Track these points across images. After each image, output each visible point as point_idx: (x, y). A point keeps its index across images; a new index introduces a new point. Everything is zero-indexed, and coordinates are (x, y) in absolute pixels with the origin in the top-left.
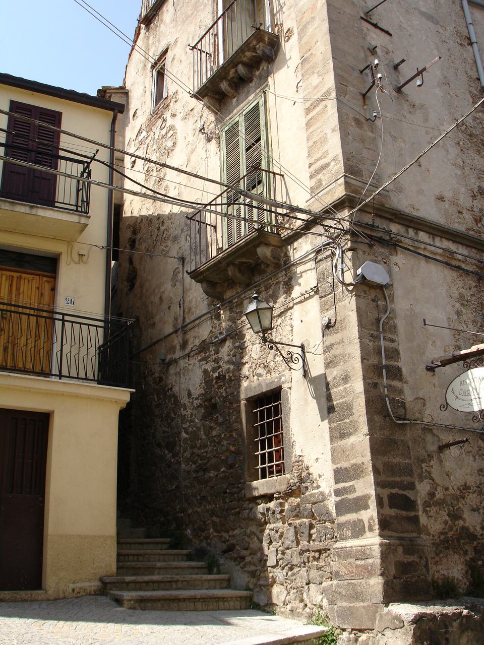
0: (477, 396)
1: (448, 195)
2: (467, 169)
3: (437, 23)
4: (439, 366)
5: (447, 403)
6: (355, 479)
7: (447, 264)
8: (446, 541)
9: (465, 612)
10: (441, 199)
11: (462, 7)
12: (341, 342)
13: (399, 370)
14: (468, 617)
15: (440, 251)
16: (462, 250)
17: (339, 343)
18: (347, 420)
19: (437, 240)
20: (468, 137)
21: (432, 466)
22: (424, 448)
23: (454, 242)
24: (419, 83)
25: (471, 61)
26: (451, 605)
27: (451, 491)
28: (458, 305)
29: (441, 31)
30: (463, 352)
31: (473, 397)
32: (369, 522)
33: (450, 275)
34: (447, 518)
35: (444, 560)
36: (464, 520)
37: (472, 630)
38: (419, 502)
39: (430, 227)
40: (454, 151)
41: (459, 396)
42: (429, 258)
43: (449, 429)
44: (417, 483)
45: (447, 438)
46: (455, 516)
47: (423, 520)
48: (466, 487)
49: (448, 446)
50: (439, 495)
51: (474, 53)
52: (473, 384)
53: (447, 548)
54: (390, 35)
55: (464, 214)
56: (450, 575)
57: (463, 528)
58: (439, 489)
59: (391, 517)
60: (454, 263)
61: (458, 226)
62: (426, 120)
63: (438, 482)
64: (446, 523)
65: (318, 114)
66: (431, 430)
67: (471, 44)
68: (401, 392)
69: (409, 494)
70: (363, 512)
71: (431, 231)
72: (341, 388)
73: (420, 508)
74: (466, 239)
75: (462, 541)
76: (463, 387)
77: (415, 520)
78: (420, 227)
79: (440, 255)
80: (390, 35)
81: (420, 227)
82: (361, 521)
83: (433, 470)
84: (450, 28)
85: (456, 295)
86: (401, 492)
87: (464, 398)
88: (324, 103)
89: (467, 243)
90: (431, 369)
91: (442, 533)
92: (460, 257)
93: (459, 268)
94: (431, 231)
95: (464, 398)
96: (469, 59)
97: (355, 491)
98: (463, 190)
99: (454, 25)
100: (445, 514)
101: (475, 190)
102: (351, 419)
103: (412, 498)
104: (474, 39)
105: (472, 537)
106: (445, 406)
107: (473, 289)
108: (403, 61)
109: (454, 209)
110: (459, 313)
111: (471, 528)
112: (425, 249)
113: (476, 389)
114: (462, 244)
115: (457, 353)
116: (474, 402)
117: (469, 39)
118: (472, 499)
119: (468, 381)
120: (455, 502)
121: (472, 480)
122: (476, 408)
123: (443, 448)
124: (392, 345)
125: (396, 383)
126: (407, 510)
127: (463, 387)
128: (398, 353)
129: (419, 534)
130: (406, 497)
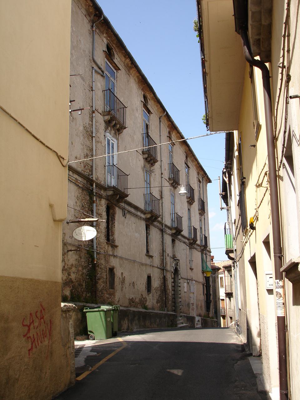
0: (84, 236)
2: (84, 145)
3: (84, 81)
4: (71, 222)
5: (73, 236)
7: (76, 184)
8: (66, 283)
9: (74, 306)
11: (92, 73)
14: (75, 307)
15: (74, 179)
16: (80, 179)
19: (74, 174)
20: (86, 132)
21: (65, 257)
23: (78, 175)
24: (79, 113)
25: (91, 98)
26: (70, 303)
27: (69, 266)
28: (76, 199)
29: (85, 84)
30: (82, 220)
31: (83, 236)
33: (76, 188)
34: (67, 275)
35: (66, 289)
36: (71, 276)
37: (76, 312)
39: (74, 170)
40: (82, 138)
41: (77, 234)
42: (72, 181)
43: (70, 244)
45: (70, 248)
46: (69, 275)
48: (72, 265)
49: (71, 251)
50: (66, 267)
51: (92, 94)
52: (83, 231)
53: (66, 285)
55: (82, 164)
56: (67, 294)
57: (71, 279)
58: (66, 265)
60: (77, 183)
61: (79, 169)
62: (76, 125)
63: (66, 262)
64: (67, 276)
66: (66, 245)
67: (92, 90)
71: (73, 171)
74: (82, 175)
75: (70, 283)
76: (80, 232)
78: (71, 170)
79: (74, 180)
81: (71, 170)
83: (65, 258)
84: (87, 83)
85: (76, 196)
87: (79, 235)
89: (82, 176)
90: (68, 223)
91: (65, 280)
92: (79, 181)
93: (78, 185)
94: (73, 171)
95: (79, 235)
96: (90, 97)
98: (82, 154)
99: (89, 81)
100: (67, 273)
101: (86, 155)
104: (94, 89)
105: (72, 282)
106: (72, 237)
107: (81, 194)
108: (74, 101)
110: (76, 203)
111: (73, 279)
112: (71, 178)
113: (84, 233)
114: (80, 176)
115: (79, 220)
116: (83, 237)
117: (92, 88)
118: (74, 269)
119: (82, 230)
120: (69, 270)
121: (74, 263)
122: (84, 240)
123: (68, 251)
127: (80, 232)
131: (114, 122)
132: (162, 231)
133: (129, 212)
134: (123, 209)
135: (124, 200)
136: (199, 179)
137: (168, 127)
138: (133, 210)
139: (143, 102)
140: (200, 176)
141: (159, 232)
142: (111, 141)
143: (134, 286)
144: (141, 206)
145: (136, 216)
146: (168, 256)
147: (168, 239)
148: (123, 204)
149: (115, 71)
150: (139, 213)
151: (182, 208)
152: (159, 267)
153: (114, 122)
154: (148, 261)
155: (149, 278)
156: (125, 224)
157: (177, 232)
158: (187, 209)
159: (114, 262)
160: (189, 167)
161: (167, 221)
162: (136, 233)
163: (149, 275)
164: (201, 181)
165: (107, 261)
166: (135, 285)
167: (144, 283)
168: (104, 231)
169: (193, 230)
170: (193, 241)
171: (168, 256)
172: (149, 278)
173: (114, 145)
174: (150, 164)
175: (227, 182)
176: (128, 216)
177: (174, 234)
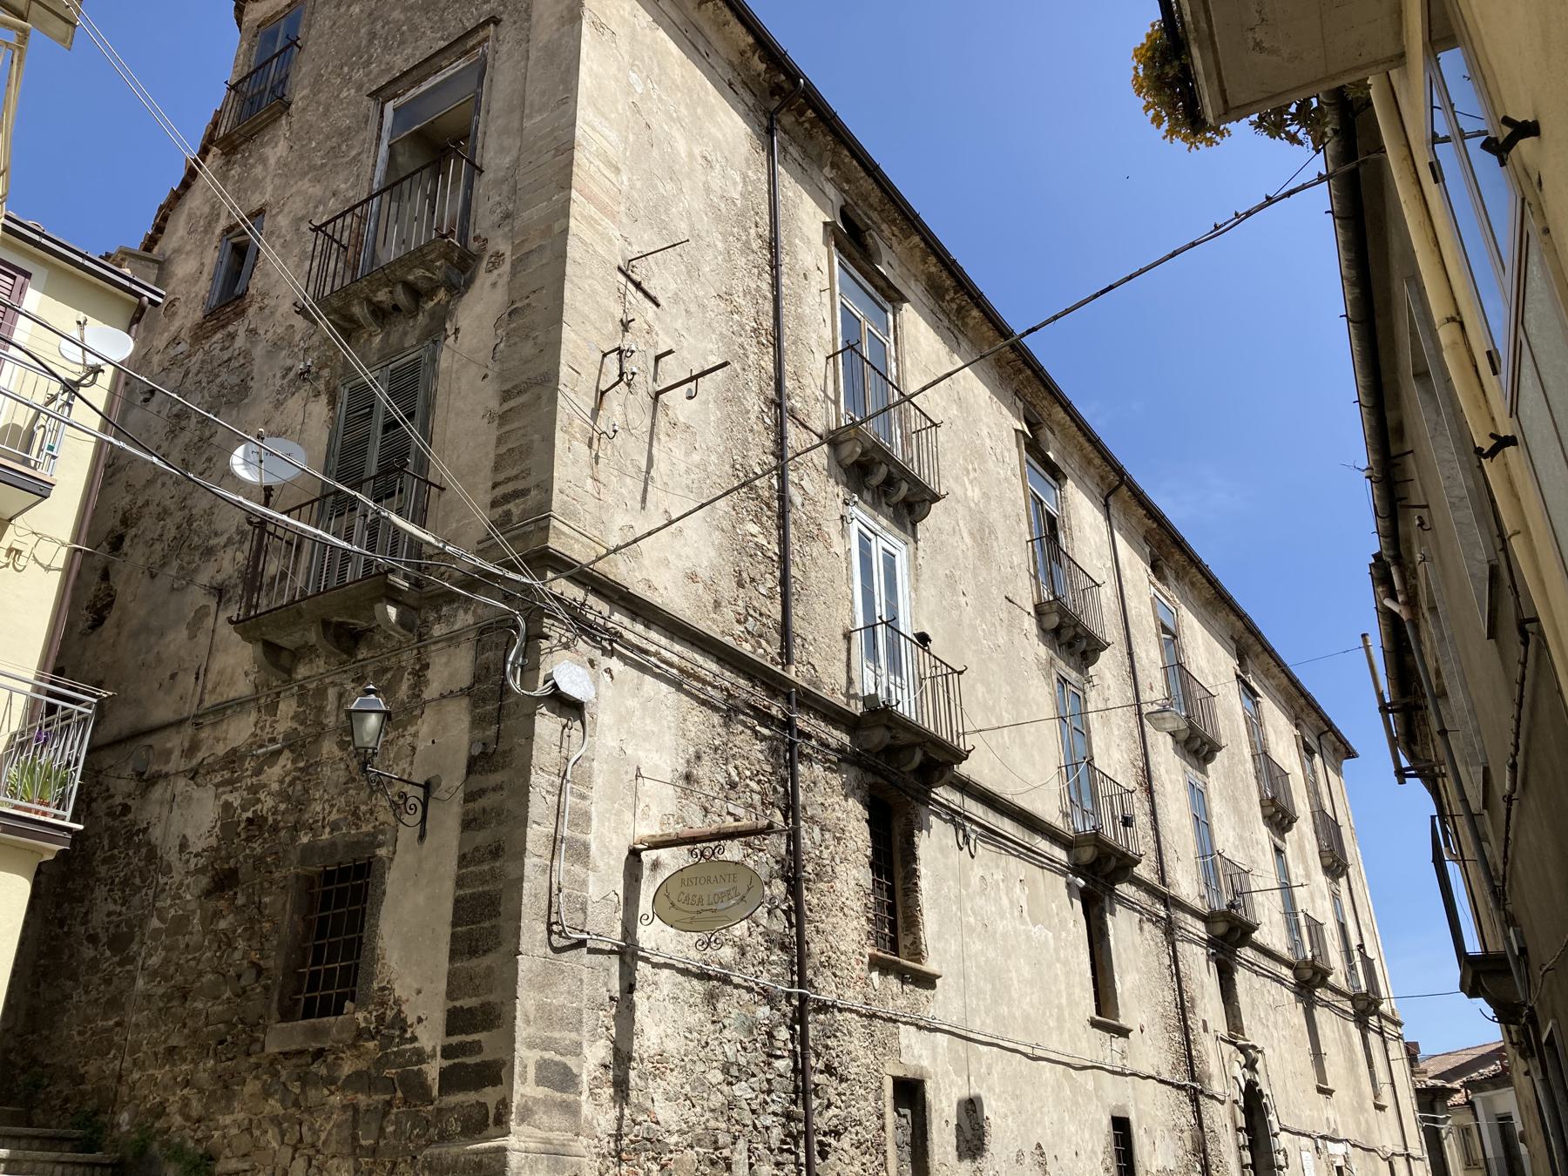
1: (704, 574)
6: (484, 1029)
10: (693, 577)
12: (498, 788)
13: (586, 846)
17: (494, 790)
18: (486, 924)
22: (606, 984)
32: (497, 1108)
38: (585, 1078)
44: (585, 1045)
47: (587, 1108)
54: (658, 305)
59: (536, 1101)
65: (523, 405)
68: (584, 883)
69: (571, 1062)
70: (489, 1090)
72: (486, 867)
73: (585, 1087)
77: (572, 1110)
80: (658, 305)
82: (483, 1105)
86: (558, 1058)
88: (536, 389)
97: (480, 1050)
102: (493, 922)
103: (575, 1070)
108: (670, 352)
109: (708, 599)
124: (583, 804)
125: (577, 868)
126: (563, 1090)
128: (590, 819)
129: (577, 1135)
130: (566, 1067)
131: (883, 470)
132: (1170, 930)
133: (991, 834)
134: (956, 818)
135: (948, 776)
136: (1304, 742)
137: (1145, 538)
138: (1007, 826)
139: (1023, 432)
140: (1306, 730)
141: (1153, 933)
142: (877, 547)
143: (1042, 1165)
144: (1049, 808)
145: (1029, 854)
146: (1206, 1030)
147: (1196, 960)
148: (943, 793)
149: (888, 307)
150: (1043, 845)
151: (1241, 835)
152: (1166, 1076)
153: (883, 470)
154: (1095, 1046)
155: (1121, 1126)
156: (975, 882)
157: (1230, 936)
158: (1269, 848)
159: (918, 1053)
160: (1255, 694)
161: (1186, 884)
162: (1035, 925)
163: (1122, 1115)
164: (1314, 746)
165: (889, 1048)
166: (1049, 1157)
167: (1093, 1151)
168: (857, 906)
169: (1304, 931)
170: (1315, 974)
171: (1206, 1030)
172: (1121, 1126)
173: (898, 559)
174: (1078, 658)
175: (1404, 616)
176: (982, 849)
177: (1224, 937)
